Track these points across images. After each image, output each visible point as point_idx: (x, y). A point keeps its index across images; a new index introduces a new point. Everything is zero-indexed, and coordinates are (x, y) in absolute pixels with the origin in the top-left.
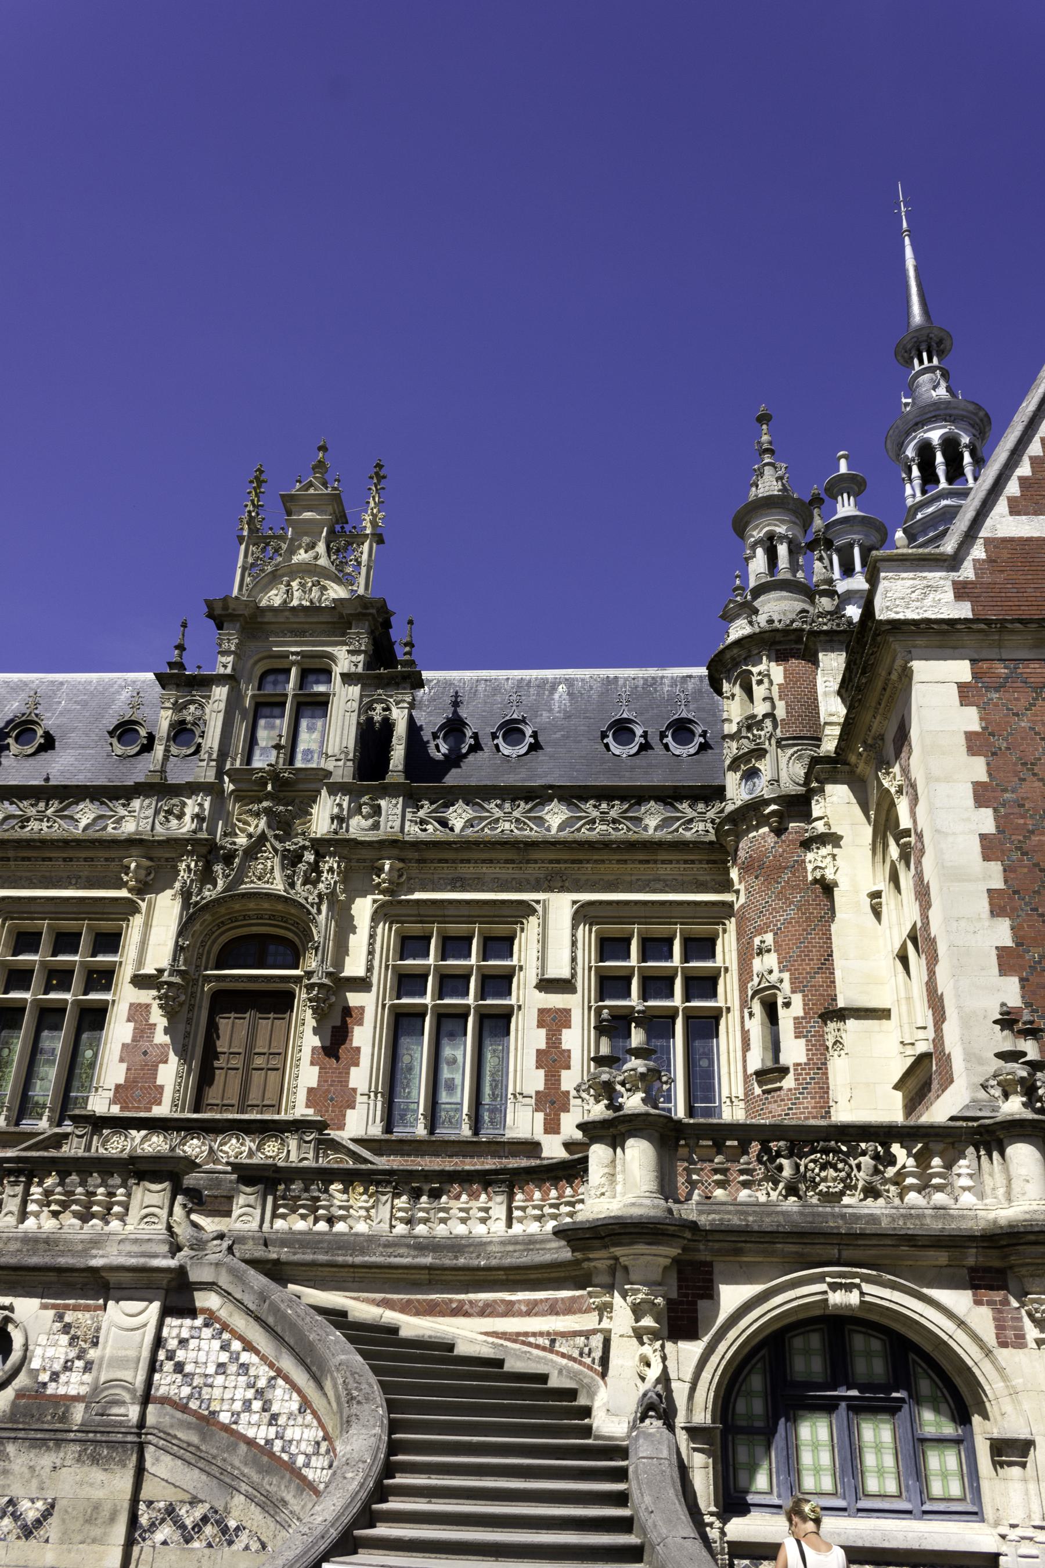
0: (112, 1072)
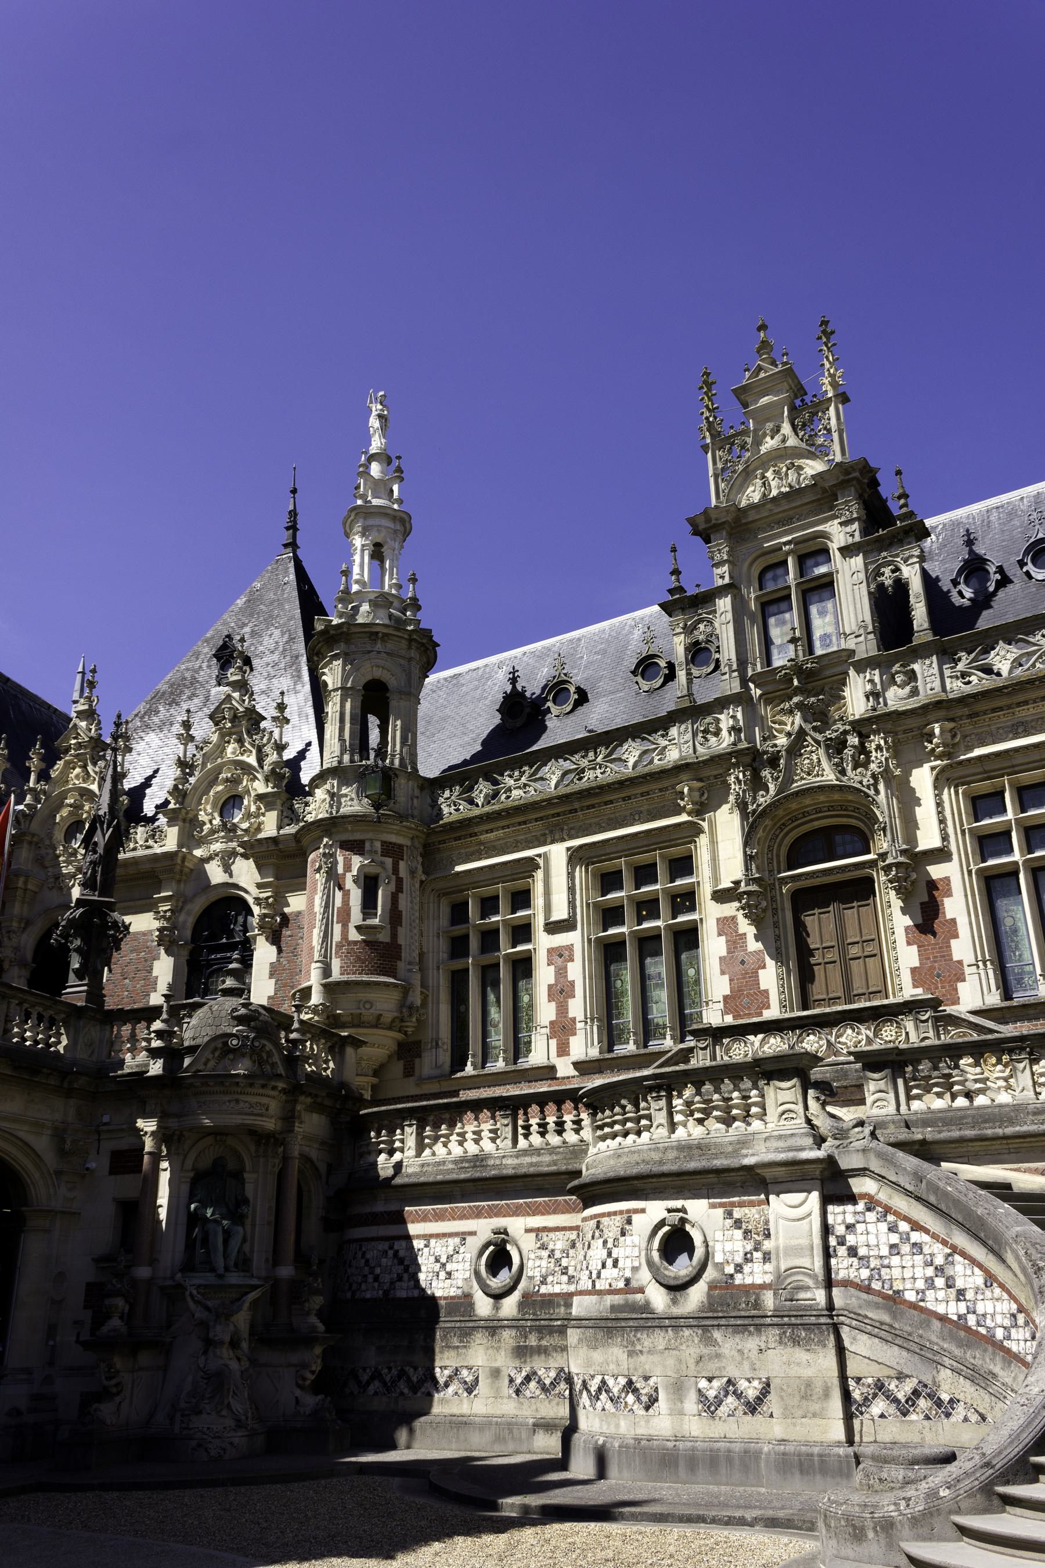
0: (716, 985)
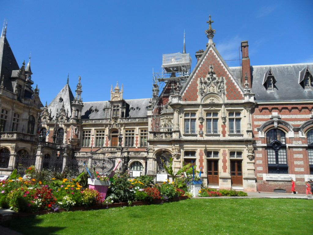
0: (105, 142)
